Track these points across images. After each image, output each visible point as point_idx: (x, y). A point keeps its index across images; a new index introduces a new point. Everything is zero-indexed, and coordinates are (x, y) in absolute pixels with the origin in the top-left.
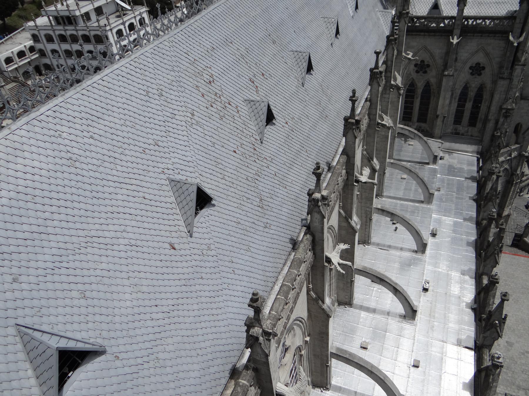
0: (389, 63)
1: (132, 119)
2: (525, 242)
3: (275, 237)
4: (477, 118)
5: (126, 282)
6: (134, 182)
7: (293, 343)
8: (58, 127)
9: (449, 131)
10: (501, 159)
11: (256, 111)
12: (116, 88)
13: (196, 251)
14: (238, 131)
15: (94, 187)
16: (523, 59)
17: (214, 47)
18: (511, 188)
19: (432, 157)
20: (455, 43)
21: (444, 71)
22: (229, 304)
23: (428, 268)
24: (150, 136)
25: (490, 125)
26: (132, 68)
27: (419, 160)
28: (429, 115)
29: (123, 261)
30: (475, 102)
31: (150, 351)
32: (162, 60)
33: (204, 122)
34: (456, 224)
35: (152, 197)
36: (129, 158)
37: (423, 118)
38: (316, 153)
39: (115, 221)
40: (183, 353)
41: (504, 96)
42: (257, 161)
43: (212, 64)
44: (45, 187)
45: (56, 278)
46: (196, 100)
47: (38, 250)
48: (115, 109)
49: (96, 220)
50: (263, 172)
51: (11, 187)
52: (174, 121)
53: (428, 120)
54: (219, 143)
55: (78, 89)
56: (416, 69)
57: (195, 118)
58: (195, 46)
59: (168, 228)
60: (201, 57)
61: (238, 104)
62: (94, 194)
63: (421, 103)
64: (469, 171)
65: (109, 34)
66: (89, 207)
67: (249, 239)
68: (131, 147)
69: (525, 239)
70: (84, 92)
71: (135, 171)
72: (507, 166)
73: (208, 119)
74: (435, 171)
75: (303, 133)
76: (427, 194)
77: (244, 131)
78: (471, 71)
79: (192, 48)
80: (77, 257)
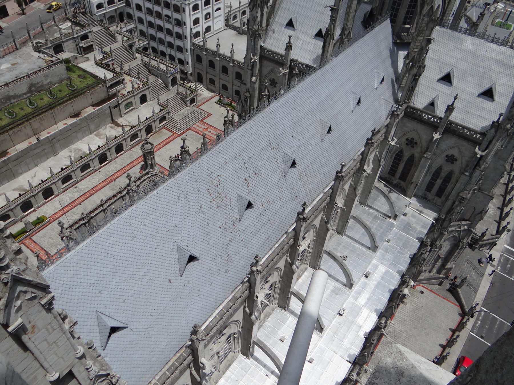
0: (365, 156)
1: (167, 213)
2: (457, 292)
3: (230, 278)
4: (443, 192)
5: (144, 297)
6: (159, 247)
7: (228, 332)
8: (131, 221)
9: (420, 194)
10: (450, 229)
11: (241, 202)
12: (163, 196)
13: (181, 284)
14: (227, 215)
15: (140, 251)
16: (483, 167)
17: (227, 161)
18: (456, 250)
19: (394, 215)
20: (435, 139)
21: (424, 153)
22: (192, 312)
23: (350, 299)
24: (174, 222)
25: (449, 203)
26: (174, 184)
27: (385, 212)
28: (408, 177)
29: (145, 287)
30: (444, 180)
31: (147, 330)
32: (192, 176)
33: (207, 211)
34: (386, 272)
35: (166, 255)
36: (160, 235)
37: (404, 177)
38: (277, 223)
39: (146, 267)
40: (161, 333)
41: (463, 187)
42: (233, 232)
43: (222, 173)
44: (120, 251)
45: (115, 293)
46: (205, 198)
47: (111, 280)
48: (160, 209)
49: (138, 267)
50: (235, 239)
51: (106, 251)
52: (189, 212)
53: (407, 181)
54: (212, 223)
55: (144, 200)
56: (406, 142)
57: (202, 209)
58: (215, 163)
59: (170, 271)
60: (216, 170)
61: (232, 197)
62: (139, 254)
63: (405, 167)
64: (421, 232)
65: (187, 8)
66: (136, 260)
67: (213, 279)
68: (163, 229)
69: (459, 289)
70: (147, 201)
71: (162, 241)
72: (456, 235)
73: (209, 209)
74: (392, 225)
75: (273, 211)
76: (374, 246)
77: (231, 214)
78: (446, 158)
79: (212, 165)
80: (125, 284)
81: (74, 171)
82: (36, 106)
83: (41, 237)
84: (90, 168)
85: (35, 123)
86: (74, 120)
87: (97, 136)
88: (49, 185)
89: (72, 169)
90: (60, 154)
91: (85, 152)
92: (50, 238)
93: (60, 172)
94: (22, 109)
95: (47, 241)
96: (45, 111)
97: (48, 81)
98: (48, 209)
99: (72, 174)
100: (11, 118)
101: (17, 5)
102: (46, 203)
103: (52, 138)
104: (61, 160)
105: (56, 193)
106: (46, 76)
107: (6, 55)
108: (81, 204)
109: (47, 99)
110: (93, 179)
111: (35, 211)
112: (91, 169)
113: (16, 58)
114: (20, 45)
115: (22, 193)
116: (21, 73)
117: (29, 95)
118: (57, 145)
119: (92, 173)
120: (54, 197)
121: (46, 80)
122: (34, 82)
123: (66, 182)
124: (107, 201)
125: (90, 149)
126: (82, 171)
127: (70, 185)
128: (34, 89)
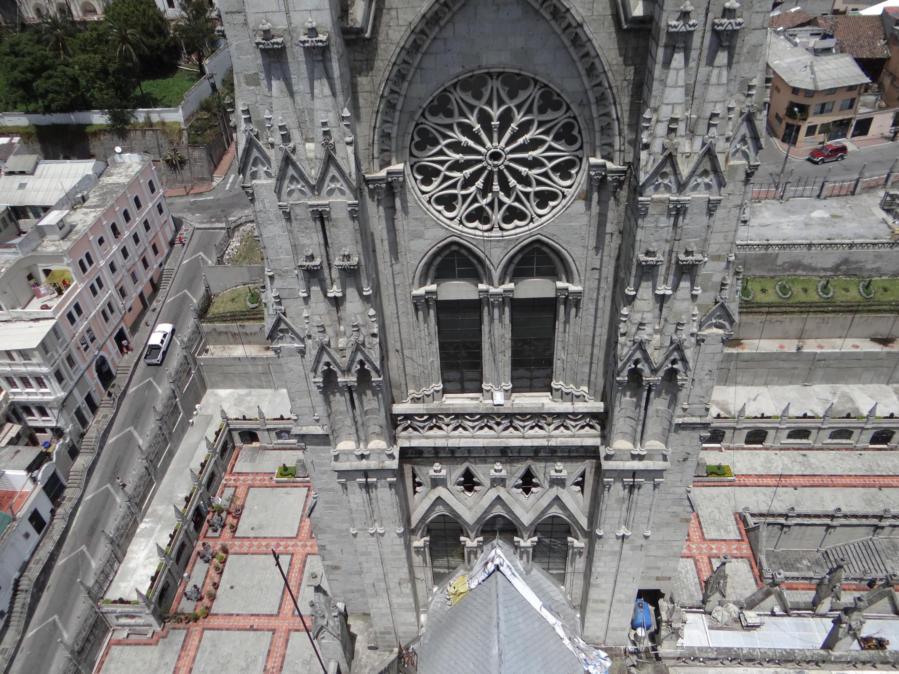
81: (820, 429)
82: (829, 296)
83: (705, 498)
84: (849, 438)
85: (812, 321)
86: (877, 348)
87: (896, 393)
88: (767, 428)
89: (820, 425)
90: (814, 387)
91: (858, 409)
92: (719, 509)
93: (797, 418)
94: (805, 290)
95: (710, 510)
96: (839, 312)
97: (874, 266)
98: (742, 460)
99: (814, 432)
100: (781, 297)
101: (891, 122)
102: (744, 449)
103: (821, 358)
104: (813, 399)
105: (767, 443)
106: (879, 257)
107: (831, 196)
108: (796, 489)
109: (854, 294)
110: (841, 459)
111: (720, 449)
112: (848, 441)
113: (843, 207)
114: (863, 189)
115: (723, 414)
116: (840, 236)
117: (829, 273)
118: (820, 373)
119: (847, 449)
120: (760, 449)
121: (875, 262)
122: (853, 259)
123: (795, 438)
124: (845, 516)
125: (873, 411)
126: (832, 437)
127: (797, 446)
128: (846, 268)
